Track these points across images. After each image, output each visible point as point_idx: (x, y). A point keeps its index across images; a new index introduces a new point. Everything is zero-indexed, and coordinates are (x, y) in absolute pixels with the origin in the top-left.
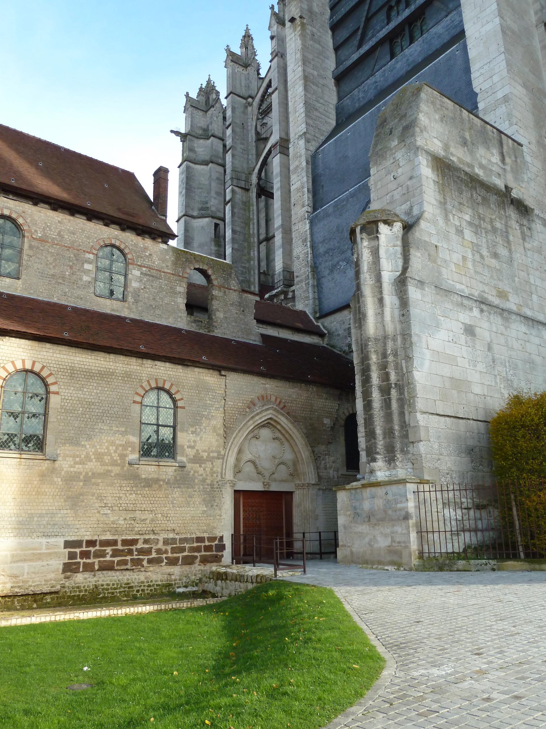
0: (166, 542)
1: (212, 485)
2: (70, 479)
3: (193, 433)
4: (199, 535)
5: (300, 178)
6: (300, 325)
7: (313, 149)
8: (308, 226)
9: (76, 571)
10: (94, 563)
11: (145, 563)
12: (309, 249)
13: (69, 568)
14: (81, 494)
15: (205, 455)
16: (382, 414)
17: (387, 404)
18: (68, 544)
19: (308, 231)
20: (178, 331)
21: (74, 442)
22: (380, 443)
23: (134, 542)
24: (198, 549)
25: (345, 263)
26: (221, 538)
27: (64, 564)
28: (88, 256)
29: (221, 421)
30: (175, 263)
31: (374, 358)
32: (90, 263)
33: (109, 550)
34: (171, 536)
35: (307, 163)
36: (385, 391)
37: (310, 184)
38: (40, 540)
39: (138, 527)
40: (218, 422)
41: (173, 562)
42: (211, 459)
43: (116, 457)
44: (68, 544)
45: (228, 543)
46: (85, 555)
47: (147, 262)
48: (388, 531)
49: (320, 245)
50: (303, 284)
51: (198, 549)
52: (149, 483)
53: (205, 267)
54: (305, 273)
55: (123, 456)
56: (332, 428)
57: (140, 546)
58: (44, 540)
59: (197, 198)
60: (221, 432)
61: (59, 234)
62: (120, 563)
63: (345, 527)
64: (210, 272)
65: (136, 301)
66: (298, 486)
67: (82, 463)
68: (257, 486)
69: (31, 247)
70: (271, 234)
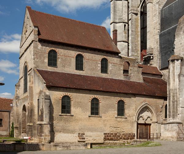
0: (123, 134)
1: (132, 122)
2: (104, 121)
3: (129, 110)
4: (130, 133)
5: (156, 19)
6: (154, 73)
7: (161, 8)
8: (158, 37)
9: (106, 140)
10: (109, 138)
11: (119, 139)
12: (159, 46)
13: (105, 139)
14: (106, 124)
15: (131, 115)
16: (172, 107)
17: (174, 105)
18: (104, 134)
19: (158, 39)
20: (121, 81)
21: (105, 113)
22: (172, 114)
23: (117, 134)
24: (129, 136)
25: (170, 52)
26: (134, 134)
27: (104, 138)
28: (99, 62)
29: (135, 107)
30: (120, 61)
31: (171, 94)
32: (99, 64)
33: (112, 135)
34: (124, 133)
35: (159, 14)
36: (173, 102)
37: (160, 22)
38: (99, 133)
39: (117, 131)
40: (134, 107)
41: (124, 139)
42: (132, 116)
43: (113, 116)
44: (104, 134)
45: (136, 135)
46: (108, 136)
47: (113, 62)
48: (172, 133)
49: (162, 45)
50: (156, 58)
51: (129, 136)
52: (119, 122)
53: (128, 61)
54: (157, 54)
55: (114, 116)
56: (162, 108)
57: (118, 135)
58: (100, 133)
59: (117, 14)
60: (135, 110)
61: (92, 57)
62: (114, 138)
63: (163, 132)
64: (129, 62)
65: (111, 73)
66: (152, 122)
67: (106, 117)
68: (143, 122)
69: (86, 62)
70: (145, 26)
